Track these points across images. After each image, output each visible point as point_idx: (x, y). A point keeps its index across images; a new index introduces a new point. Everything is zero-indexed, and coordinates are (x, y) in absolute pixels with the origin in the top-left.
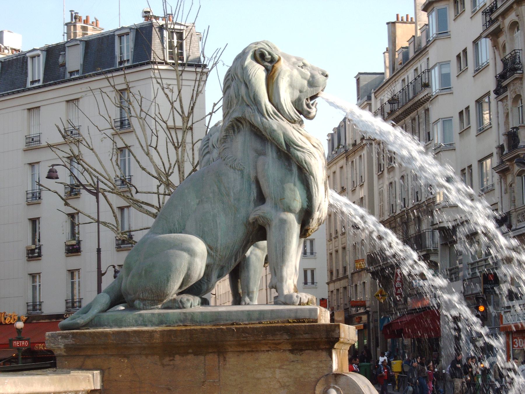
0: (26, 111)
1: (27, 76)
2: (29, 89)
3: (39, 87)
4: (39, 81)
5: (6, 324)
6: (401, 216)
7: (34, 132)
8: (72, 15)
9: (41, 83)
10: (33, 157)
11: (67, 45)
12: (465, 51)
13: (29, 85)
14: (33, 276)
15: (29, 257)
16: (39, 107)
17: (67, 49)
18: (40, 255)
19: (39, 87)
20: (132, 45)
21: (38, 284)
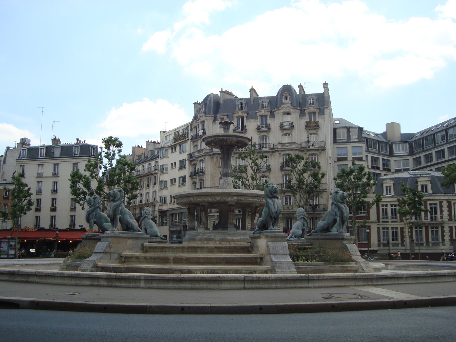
1: (39, 154)
2: (40, 159)
5: (29, 231)
6: (139, 205)
7: (40, 172)
9: (44, 157)
10: (40, 180)
12: (175, 163)
14: (37, 217)
16: (43, 164)
17: (55, 148)
18: (40, 210)
20: (79, 150)
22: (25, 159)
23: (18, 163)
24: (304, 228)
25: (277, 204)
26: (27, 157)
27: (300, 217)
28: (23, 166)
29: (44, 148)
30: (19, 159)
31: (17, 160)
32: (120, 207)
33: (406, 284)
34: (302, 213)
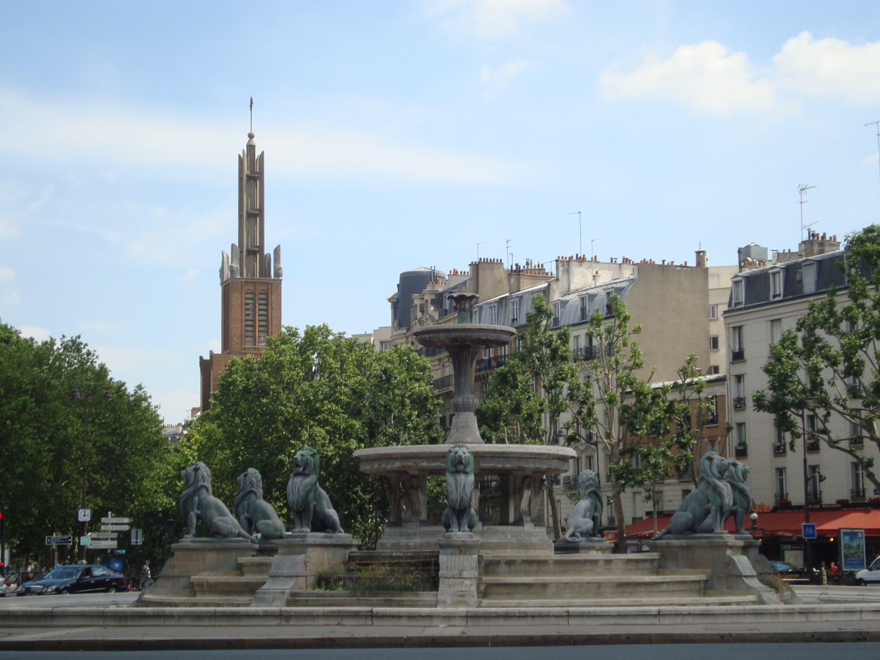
0: (769, 322)
1: (769, 291)
3: (780, 301)
4: (779, 295)
8: (809, 232)
11: (803, 264)
13: (771, 299)
15: (776, 453)
19: (780, 301)
21: (784, 477)
22: (741, 309)
23: (730, 320)
24: (596, 514)
25: (297, 487)
26: (746, 302)
27: (588, 491)
28: (740, 328)
29: (779, 272)
30: (730, 308)
31: (725, 312)
32: (196, 498)
33: (177, 626)
34: (591, 482)
